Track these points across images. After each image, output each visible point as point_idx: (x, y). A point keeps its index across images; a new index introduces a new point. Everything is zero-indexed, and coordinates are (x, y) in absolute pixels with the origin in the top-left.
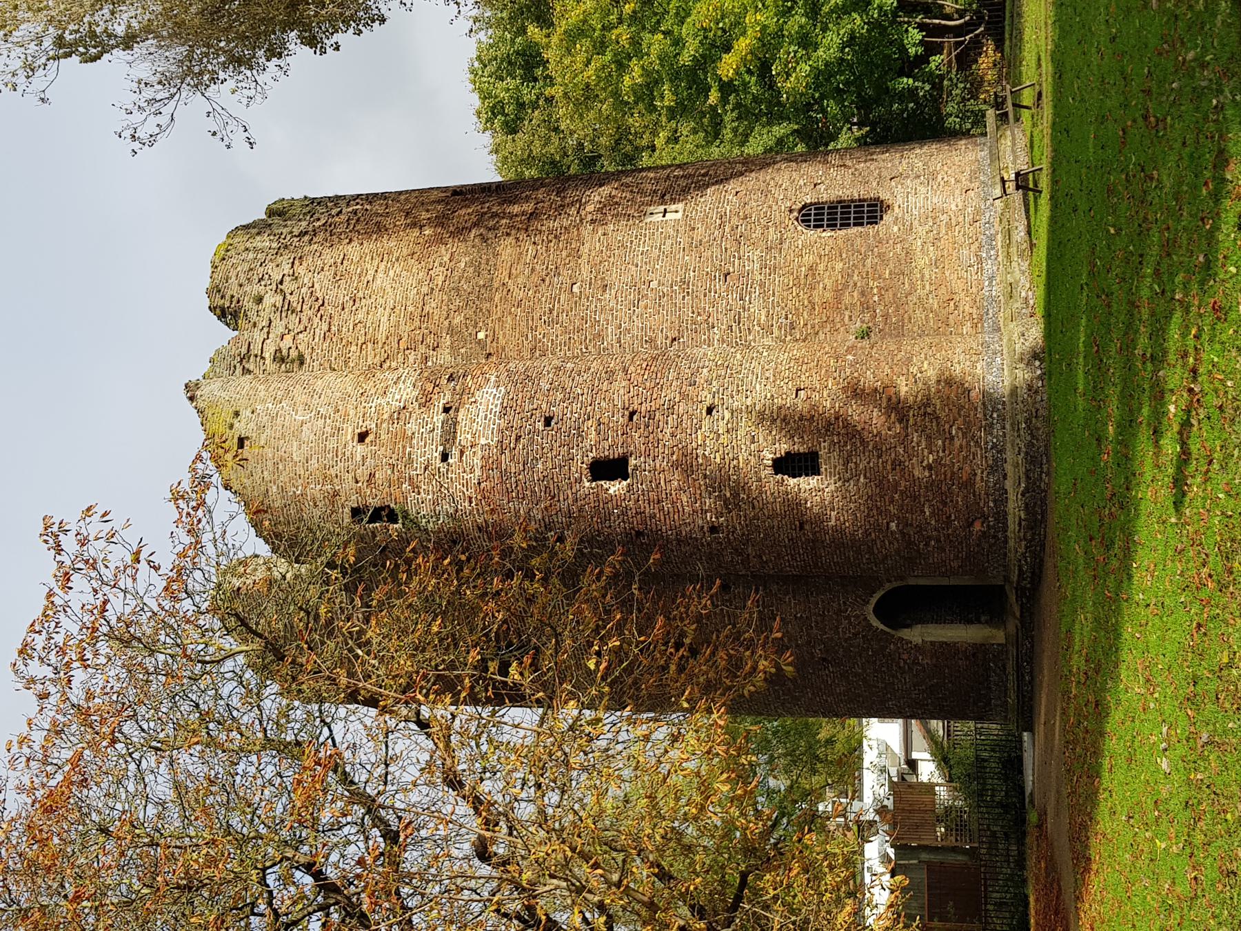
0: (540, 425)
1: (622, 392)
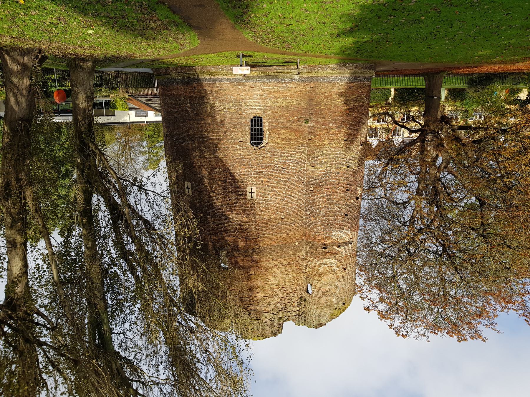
0: (347, 217)
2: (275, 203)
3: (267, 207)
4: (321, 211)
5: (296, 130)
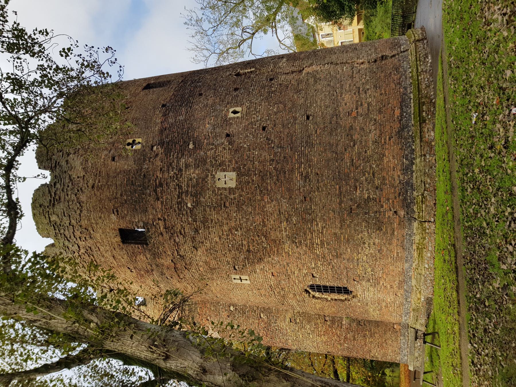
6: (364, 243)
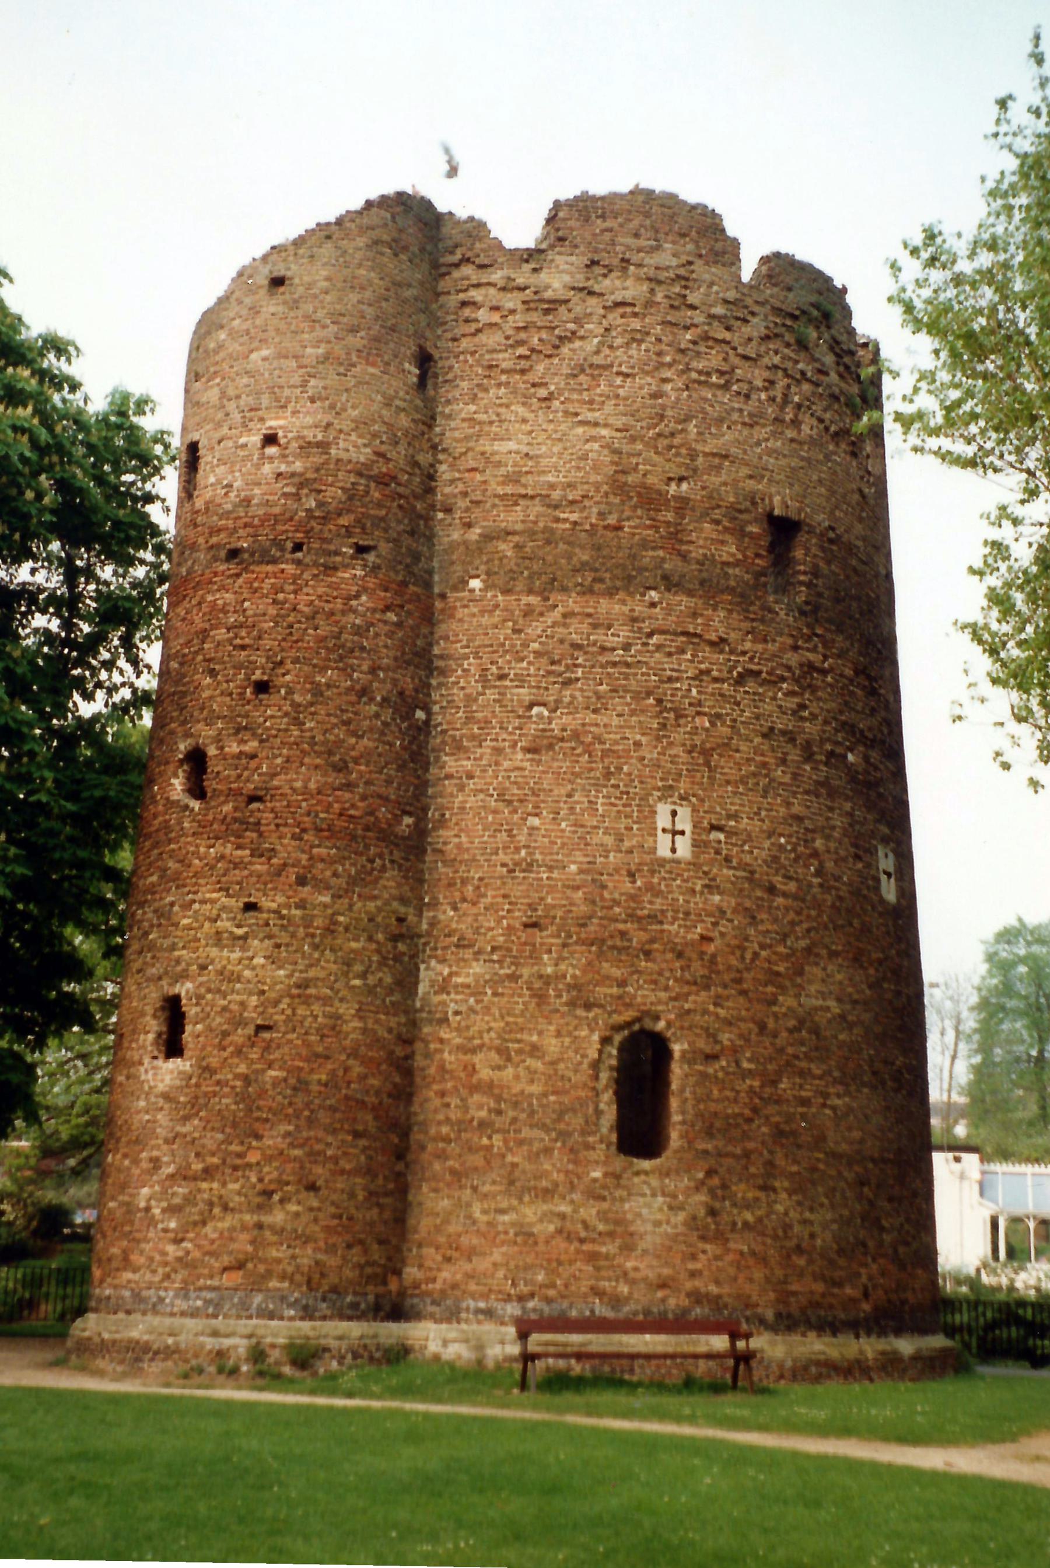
0: (258, 675)
1: (298, 784)
2: (577, 775)
3: (612, 763)
4: (377, 716)
5: (474, 1089)
6: (811, 1209)
